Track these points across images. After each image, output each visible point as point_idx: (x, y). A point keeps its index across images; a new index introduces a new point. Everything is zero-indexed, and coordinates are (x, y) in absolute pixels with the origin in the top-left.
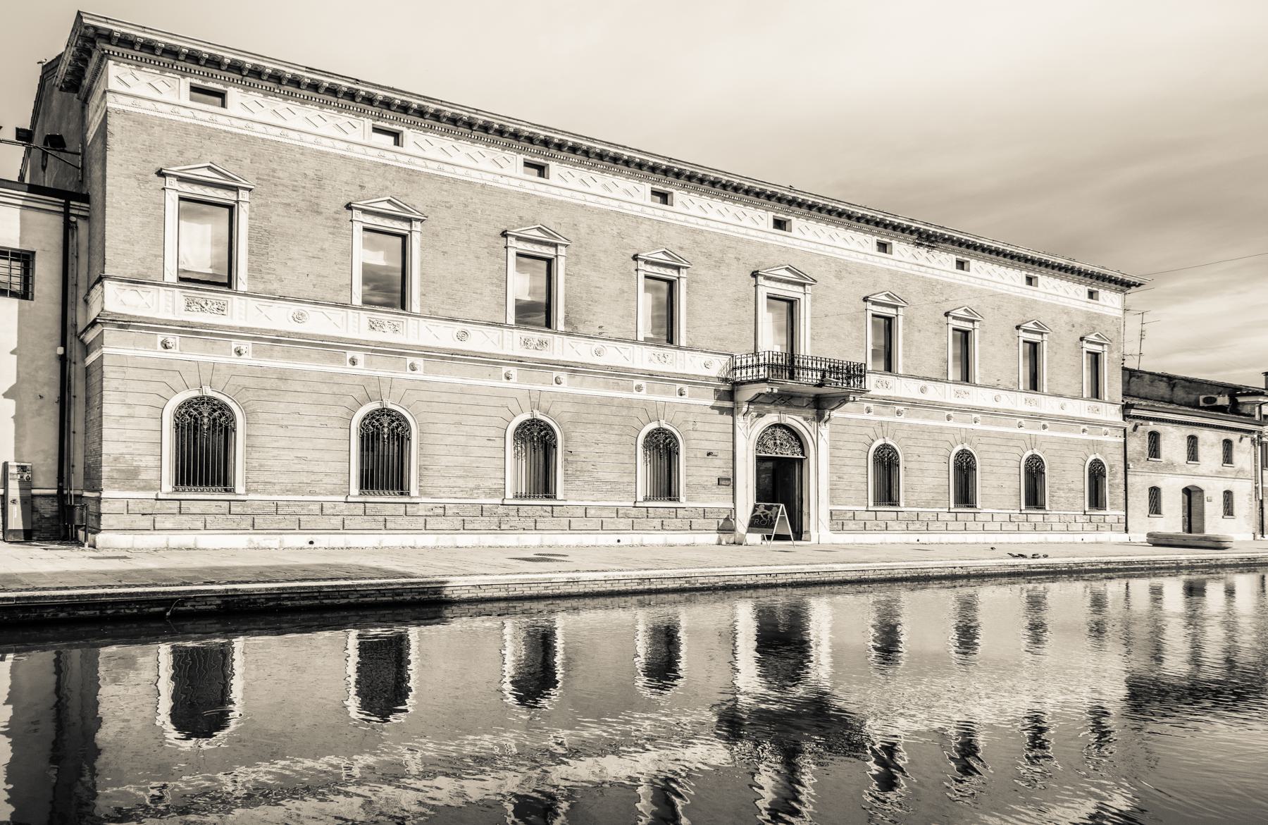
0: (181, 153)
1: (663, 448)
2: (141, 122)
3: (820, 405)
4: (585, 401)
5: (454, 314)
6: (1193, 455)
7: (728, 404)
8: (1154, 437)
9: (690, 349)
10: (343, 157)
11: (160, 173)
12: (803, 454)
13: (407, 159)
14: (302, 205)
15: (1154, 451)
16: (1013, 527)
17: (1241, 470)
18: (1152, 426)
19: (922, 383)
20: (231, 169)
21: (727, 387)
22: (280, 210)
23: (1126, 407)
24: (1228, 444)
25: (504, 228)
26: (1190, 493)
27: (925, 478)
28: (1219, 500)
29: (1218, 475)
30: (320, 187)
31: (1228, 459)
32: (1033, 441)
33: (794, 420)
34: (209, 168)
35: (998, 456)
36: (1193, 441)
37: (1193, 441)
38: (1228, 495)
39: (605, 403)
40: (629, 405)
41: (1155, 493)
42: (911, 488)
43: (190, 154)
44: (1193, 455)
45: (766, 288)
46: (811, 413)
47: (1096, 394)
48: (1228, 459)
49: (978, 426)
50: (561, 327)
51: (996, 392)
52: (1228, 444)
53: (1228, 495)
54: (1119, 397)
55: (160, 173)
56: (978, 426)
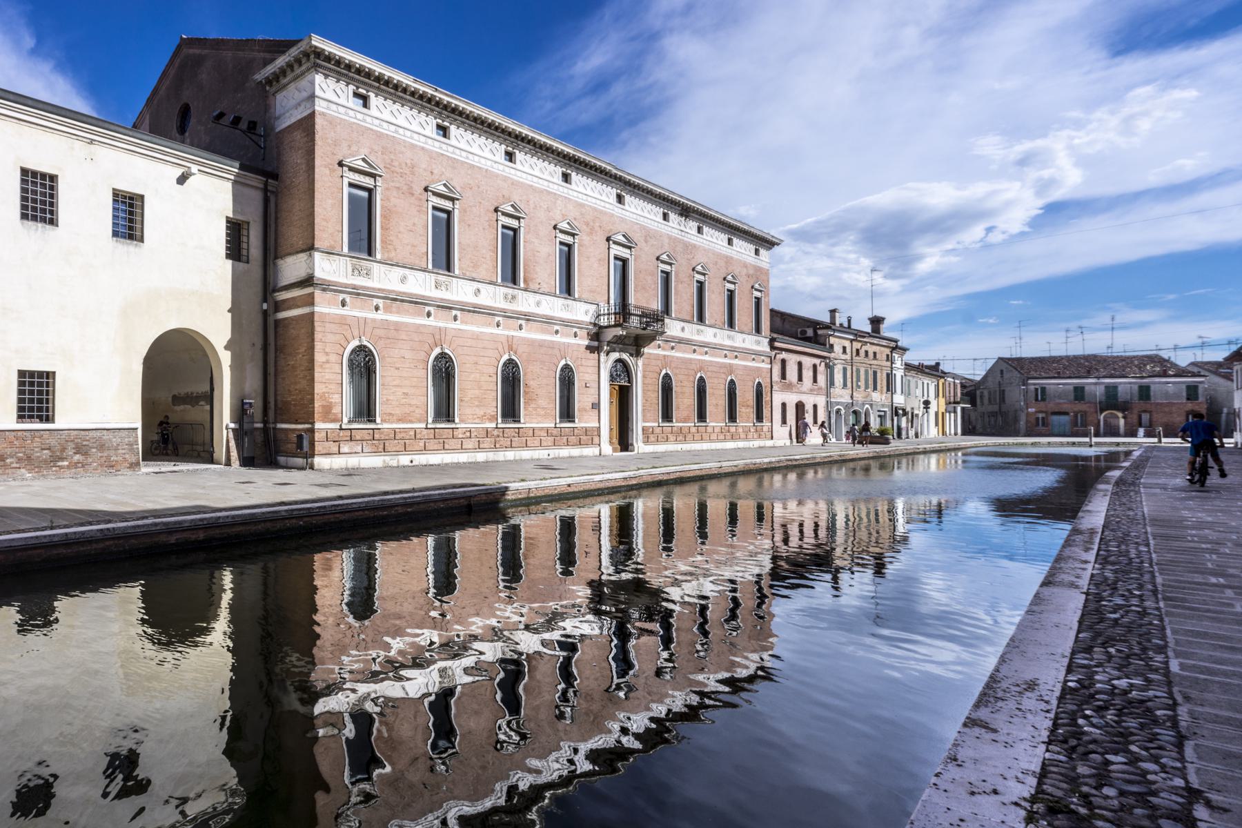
0: (350, 146)
1: (567, 380)
2: (332, 122)
3: (636, 344)
4: (532, 343)
5: (474, 275)
6: (800, 379)
7: (596, 344)
8: (783, 362)
10: (423, 148)
11: (341, 164)
12: (630, 381)
13: (451, 149)
14: (405, 188)
15: (783, 376)
16: (722, 437)
17: (820, 388)
18: (784, 355)
19: (682, 324)
20: (371, 159)
21: (595, 330)
22: (395, 193)
23: (772, 341)
24: (815, 366)
25: (496, 204)
26: (800, 407)
27: (684, 400)
28: (811, 411)
29: (811, 391)
30: (413, 174)
31: (815, 380)
32: (730, 369)
33: (625, 356)
34: (364, 160)
35: (716, 381)
36: (800, 364)
37: (800, 364)
38: (815, 407)
39: (541, 344)
40: (552, 345)
41: (784, 405)
42: (678, 408)
43: (354, 148)
44: (800, 379)
45: (616, 250)
46: (633, 349)
47: (758, 330)
48: (815, 380)
49: (707, 358)
50: (522, 285)
51: (715, 330)
52: (815, 366)
53: (815, 407)
54: (768, 333)
55: (341, 164)
56: (707, 358)
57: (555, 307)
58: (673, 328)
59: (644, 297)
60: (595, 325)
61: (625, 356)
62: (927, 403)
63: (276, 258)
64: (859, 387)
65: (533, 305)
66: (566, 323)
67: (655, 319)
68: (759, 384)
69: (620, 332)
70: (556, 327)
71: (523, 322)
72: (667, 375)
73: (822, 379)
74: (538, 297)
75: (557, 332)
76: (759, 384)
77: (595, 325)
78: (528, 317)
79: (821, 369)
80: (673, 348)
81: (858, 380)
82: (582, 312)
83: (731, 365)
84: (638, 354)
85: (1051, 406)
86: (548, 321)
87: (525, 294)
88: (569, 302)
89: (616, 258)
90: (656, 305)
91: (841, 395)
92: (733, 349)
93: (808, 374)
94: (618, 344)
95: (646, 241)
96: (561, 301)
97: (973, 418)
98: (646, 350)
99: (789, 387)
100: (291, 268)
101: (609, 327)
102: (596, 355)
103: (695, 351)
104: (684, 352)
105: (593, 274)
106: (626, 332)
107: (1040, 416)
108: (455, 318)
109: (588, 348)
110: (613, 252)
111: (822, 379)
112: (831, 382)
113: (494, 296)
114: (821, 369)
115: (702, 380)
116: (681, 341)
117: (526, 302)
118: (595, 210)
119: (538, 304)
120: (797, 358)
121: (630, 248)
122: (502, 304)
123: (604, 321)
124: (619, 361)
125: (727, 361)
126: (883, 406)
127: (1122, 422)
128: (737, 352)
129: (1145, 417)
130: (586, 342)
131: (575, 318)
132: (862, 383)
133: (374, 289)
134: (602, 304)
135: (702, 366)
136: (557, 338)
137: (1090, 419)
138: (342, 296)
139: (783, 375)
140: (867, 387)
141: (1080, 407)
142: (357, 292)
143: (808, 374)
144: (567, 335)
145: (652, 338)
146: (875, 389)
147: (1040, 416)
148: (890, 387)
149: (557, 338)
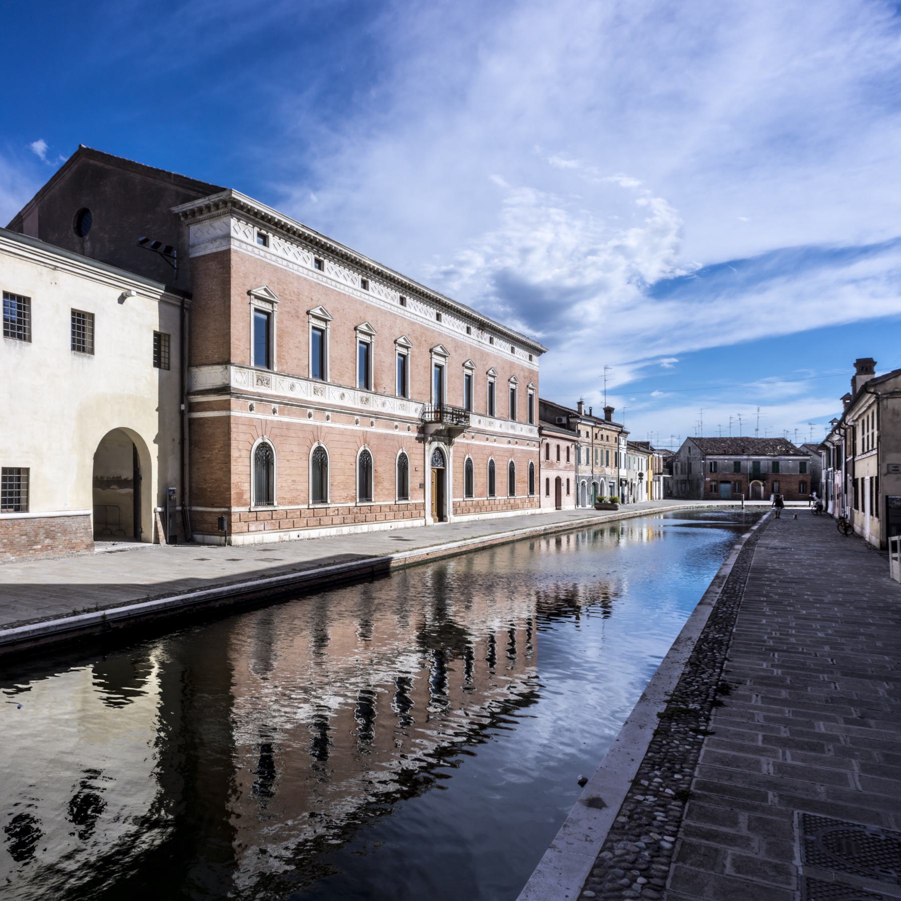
3: (449, 435)
6: (558, 459)
7: (422, 435)
9: (411, 401)
15: (547, 458)
17: (571, 466)
18: (548, 440)
24: (568, 448)
31: (568, 460)
32: (512, 452)
44: (558, 459)
48: (568, 460)
49: (495, 444)
56: (495, 444)
57: (393, 406)
58: (475, 421)
59: (454, 399)
60: (422, 420)
61: (442, 445)
62: (641, 475)
63: (190, 365)
64: (597, 463)
65: (380, 405)
66: (403, 420)
67: (463, 415)
68: (532, 464)
69: (441, 427)
70: (396, 423)
71: (373, 420)
72: (469, 460)
73: (572, 458)
74: (384, 399)
75: (396, 427)
76: (532, 464)
77: (422, 420)
78: (377, 416)
79: (572, 450)
80: (473, 437)
81: (596, 458)
82: (412, 410)
83: (513, 450)
84: (450, 443)
85: (720, 477)
86: (391, 418)
87: (376, 397)
88: (404, 402)
89: (436, 366)
90: (461, 404)
91: (585, 470)
92: (515, 437)
93: (563, 455)
94: (438, 435)
95: (456, 351)
96: (399, 402)
97: (671, 484)
98: (457, 440)
99: (551, 466)
100: (207, 376)
101: (431, 422)
102: (422, 444)
103: (487, 439)
104: (480, 440)
105: (420, 379)
106: (443, 426)
107: (713, 483)
108: (328, 418)
109: (417, 438)
110: (434, 361)
111: (572, 458)
112: (579, 461)
113: (353, 399)
114: (572, 450)
115: (492, 462)
116: (480, 432)
117: (376, 404)
118: (422, 327)
119: (384, 404)
120: (558, 442)
121: (445, 357)
122: (359, 406)
123: (428, 417)
124: (438, 449)
125: (510, 446)
126: (613, 478)
127: (762, 488)
128: (517, 439)
129: (776, 485)
130: (416, 435)
131: (408, 415)
132: (599, 461)
133: (272, 396)
134: (427, 404)
135: (493, 451)
136: (396, 432)
137: (744, 486)
138: (251, 402)
139: (547, 458)
140: (602, 464)
141: (738, 477)
142: (261, 399)
143: (563, 455)
144: (403, 429)
145: (461, 431)
146: (607, 465)
147: (713, 483)
148: (617, 464)
149: (396, 432)
